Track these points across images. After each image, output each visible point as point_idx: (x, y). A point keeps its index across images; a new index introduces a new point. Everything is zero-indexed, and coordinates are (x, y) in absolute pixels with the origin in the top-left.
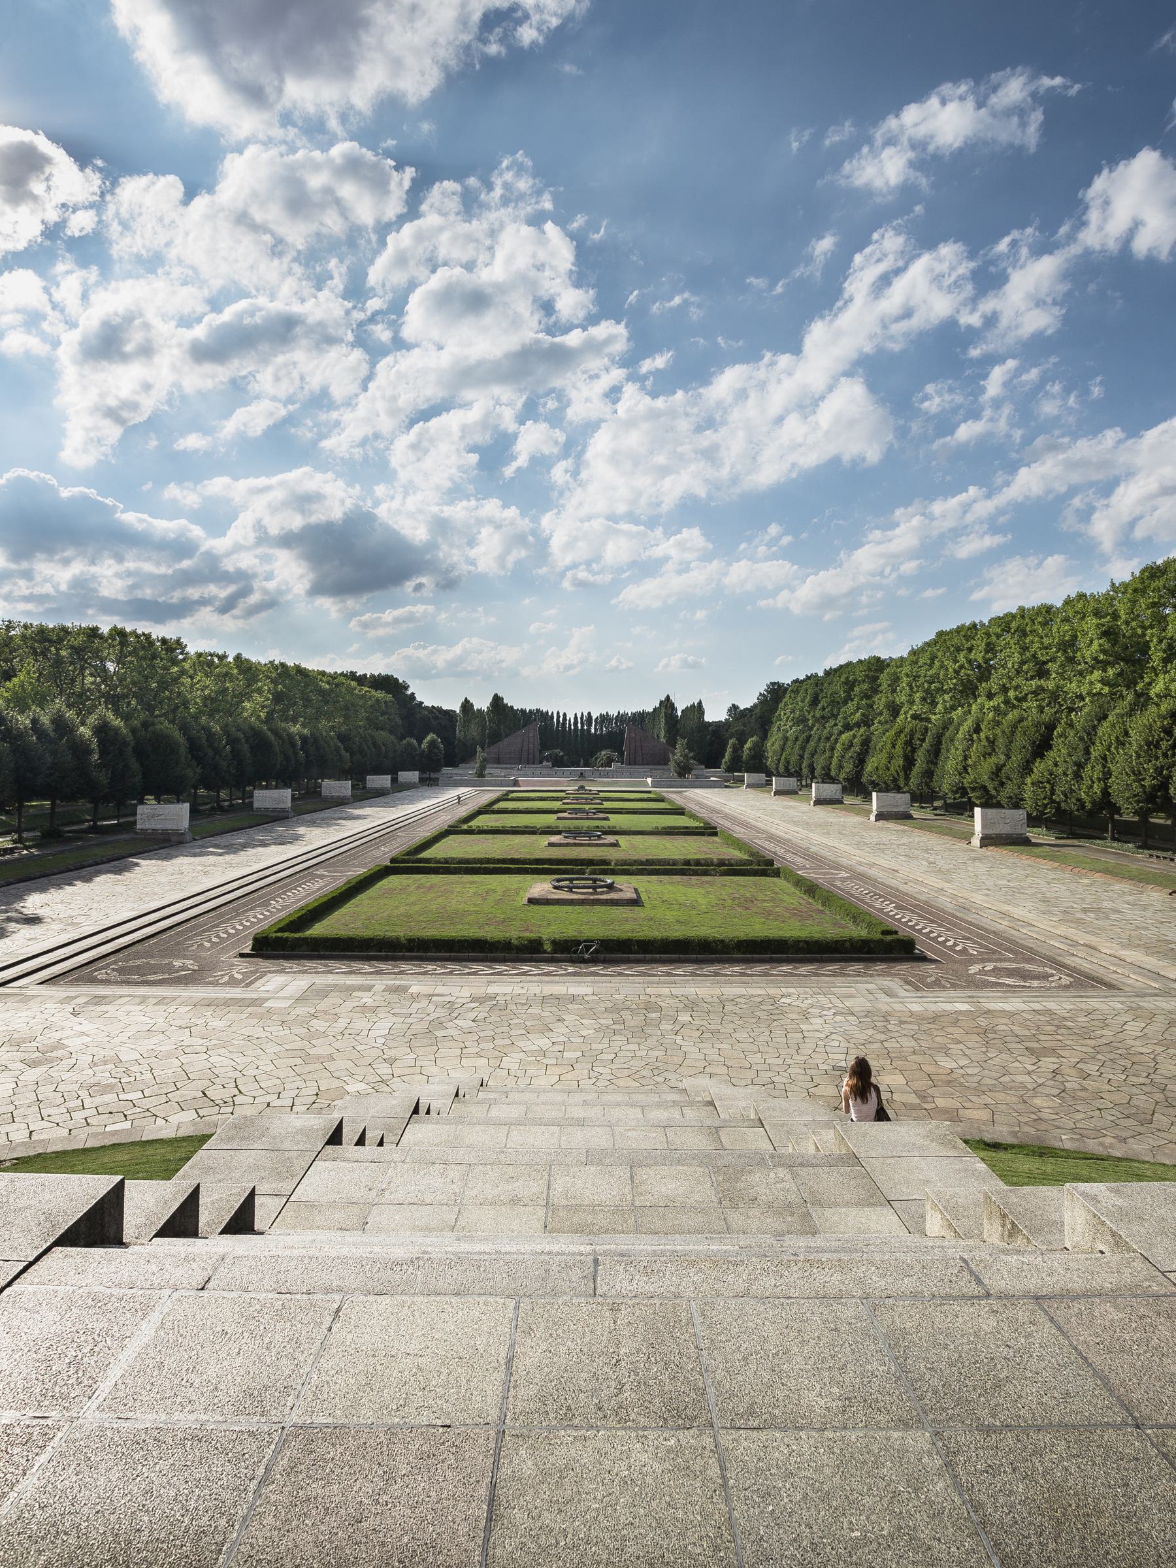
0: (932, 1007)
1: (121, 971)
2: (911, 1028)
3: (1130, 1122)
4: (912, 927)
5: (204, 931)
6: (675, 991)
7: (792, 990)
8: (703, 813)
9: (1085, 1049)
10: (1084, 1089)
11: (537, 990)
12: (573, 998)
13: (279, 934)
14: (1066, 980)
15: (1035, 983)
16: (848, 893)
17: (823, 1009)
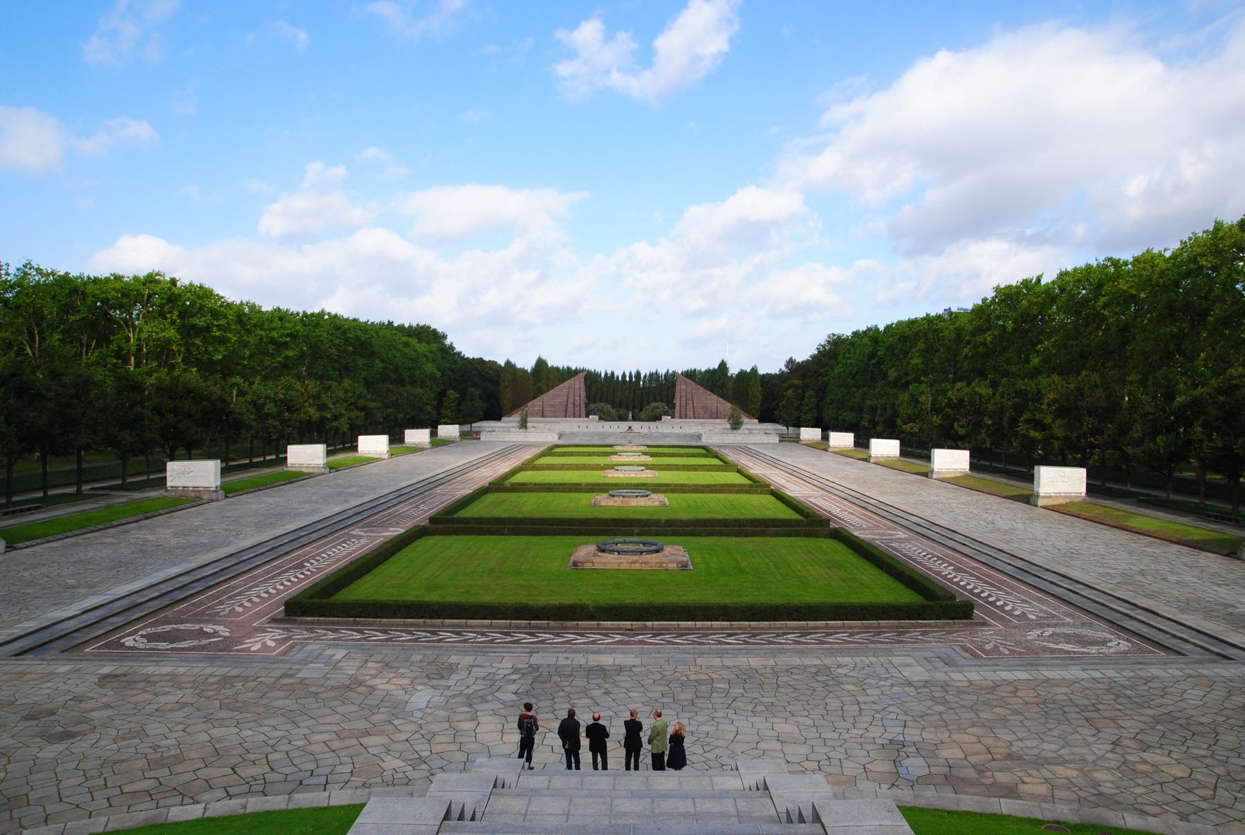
0: (990, 676)
1: (150, 638)
2: (967, 700)
3: (1190, 797)
4: (971, 591)
5: (235, 595)
6: (728, 661)
7: (849, 659)
9: (1143, 719)
10: (1145, 762)
11: (583, 662)
12: (620, 670)
14: (1124, 645)
15: (1093, 650)
17: (881, 679)
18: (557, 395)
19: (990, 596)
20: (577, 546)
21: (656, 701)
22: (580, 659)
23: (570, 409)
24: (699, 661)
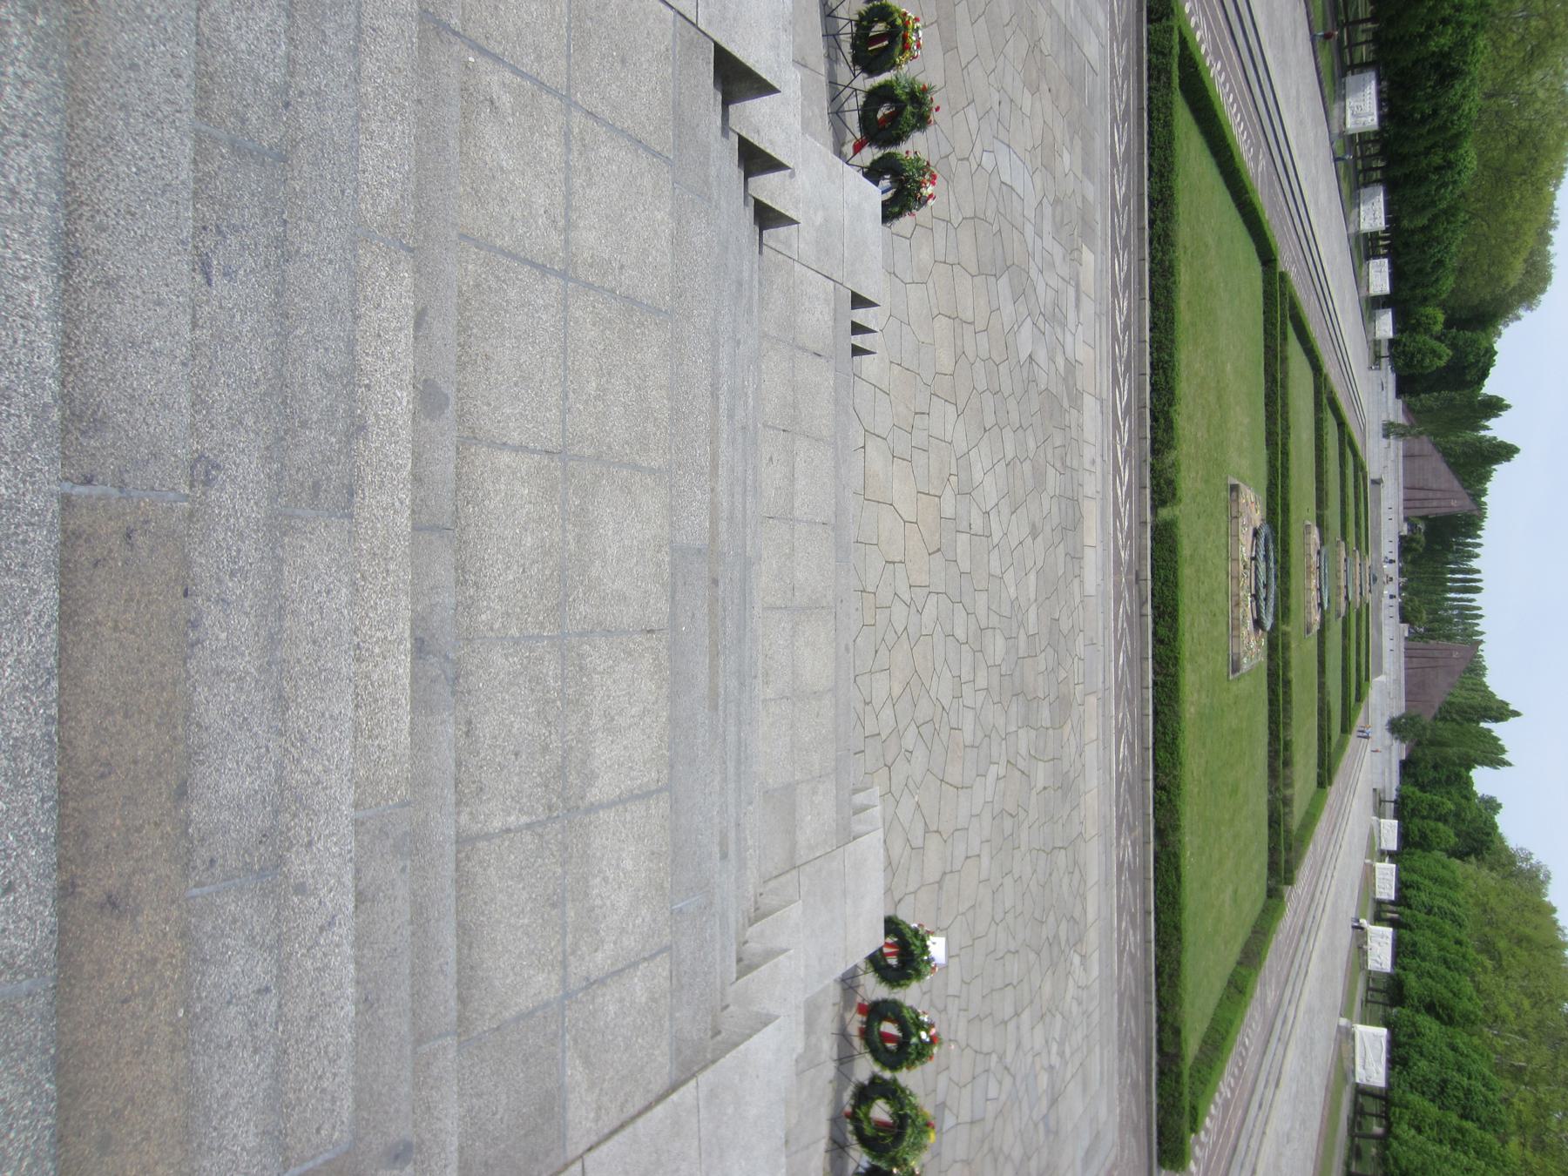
6: (1091, 752)
12: (1075, 557)
18: (1440, 475)
20: (1257, 491)
21: (1021, 624)
22: (1092, 485)
23: (1421, 494)
24: (1092, 700)
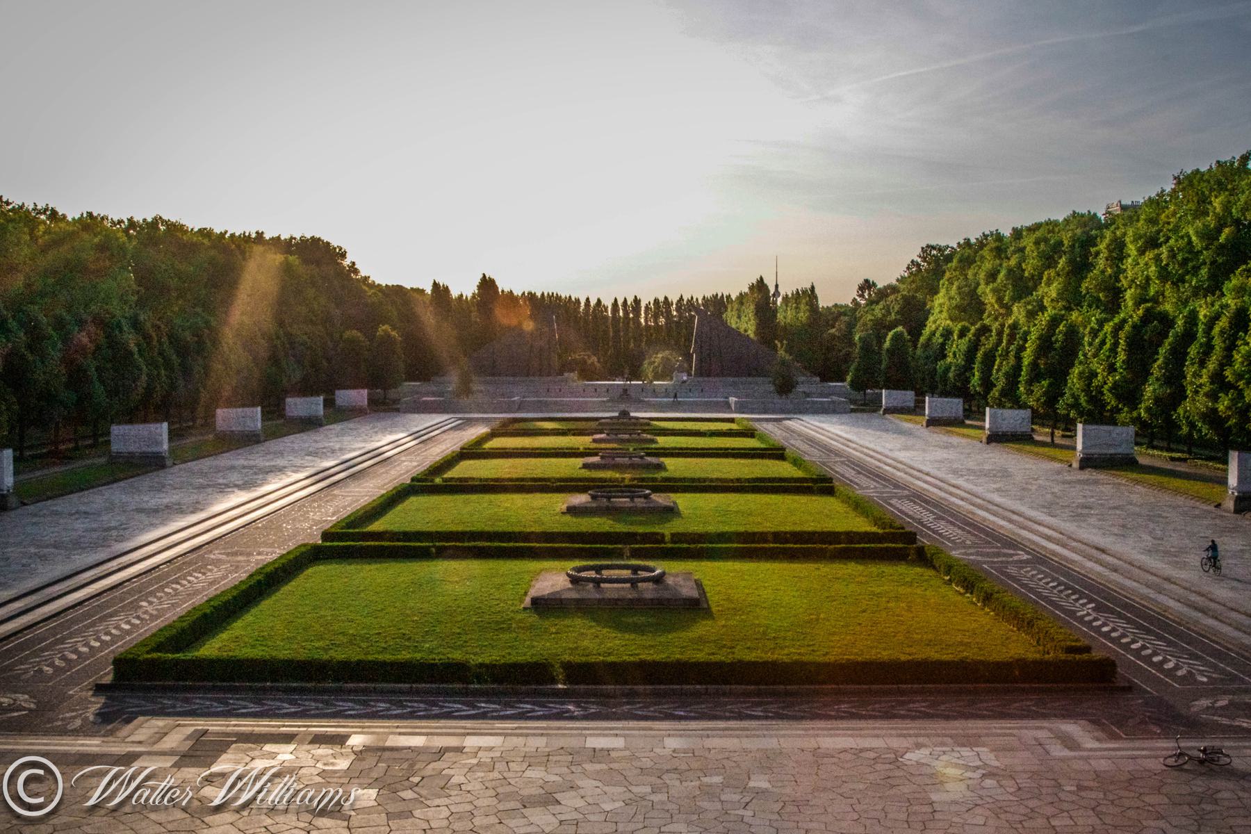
5: (43, 650)
8: (813, 456)
13: (155, 655)
16: (1025, 586)
19: (1144, 647)
